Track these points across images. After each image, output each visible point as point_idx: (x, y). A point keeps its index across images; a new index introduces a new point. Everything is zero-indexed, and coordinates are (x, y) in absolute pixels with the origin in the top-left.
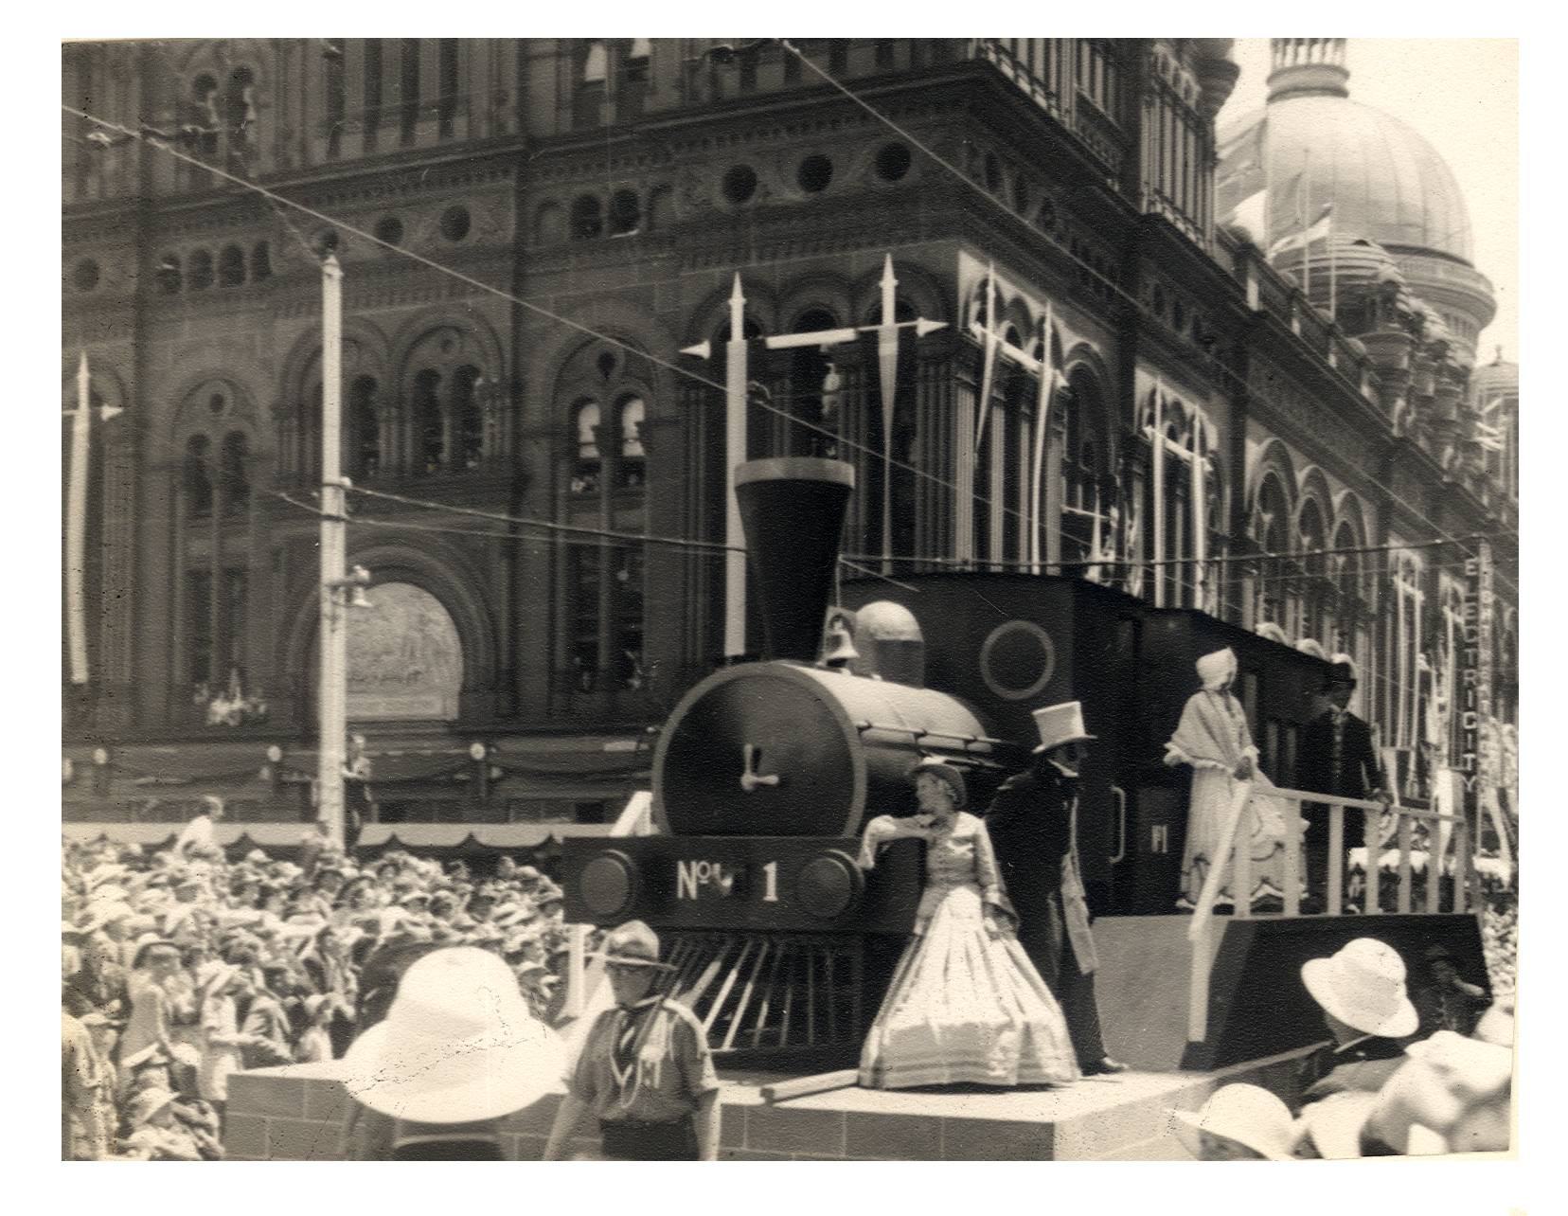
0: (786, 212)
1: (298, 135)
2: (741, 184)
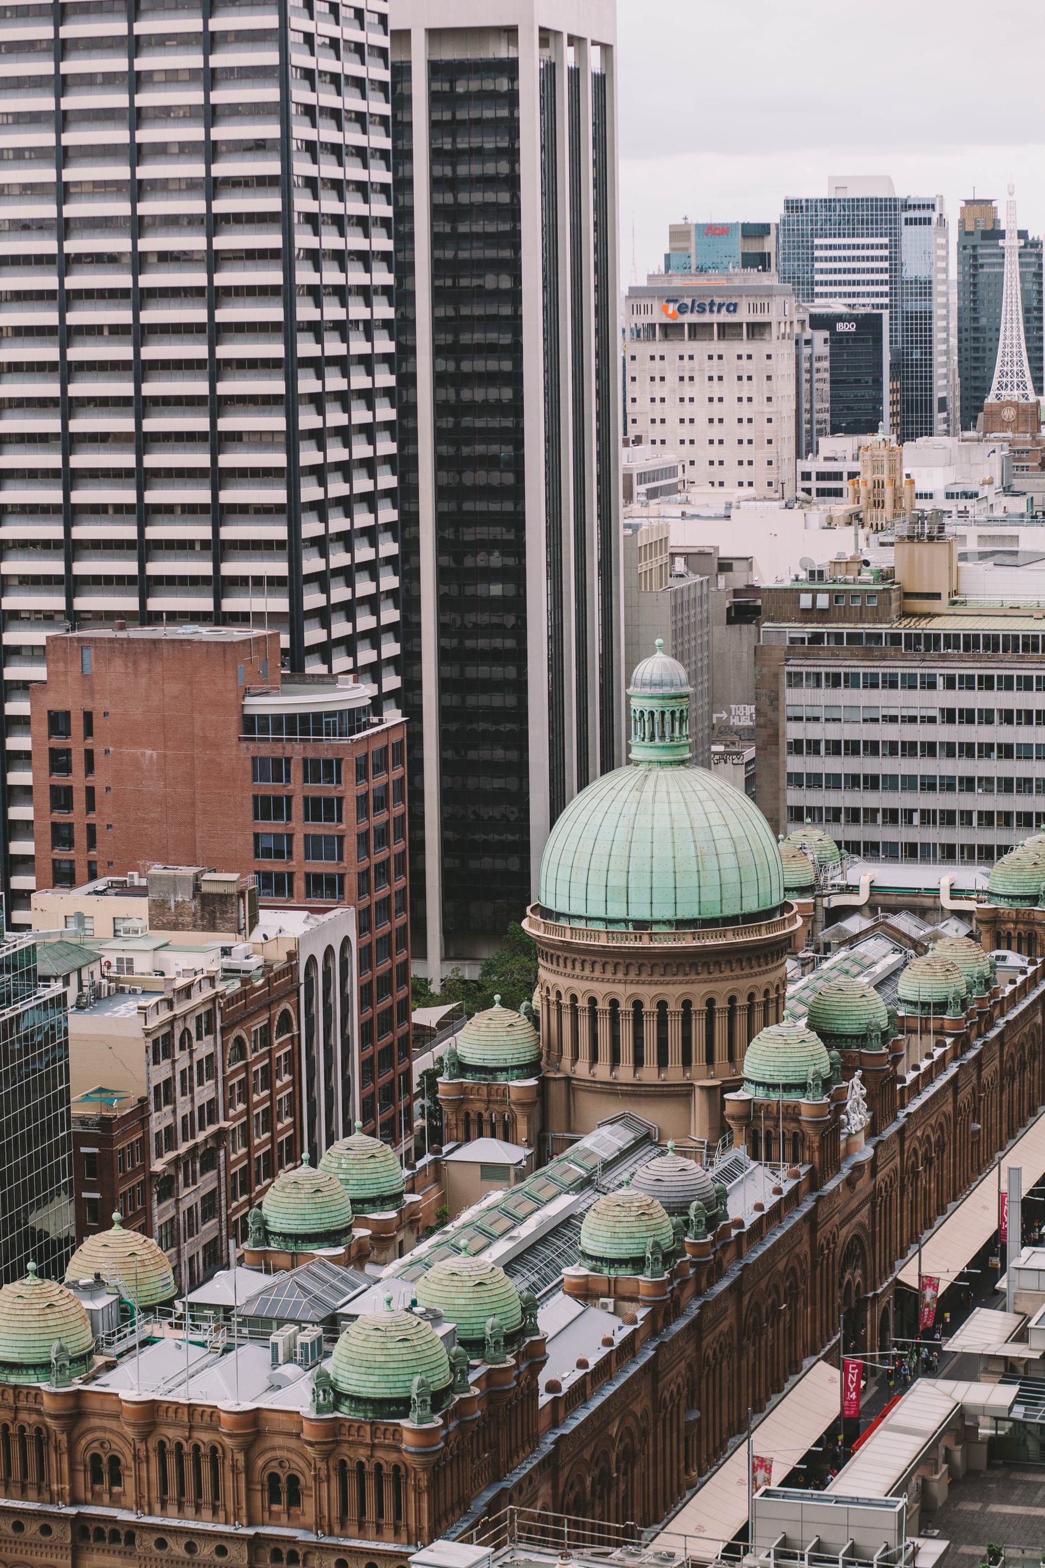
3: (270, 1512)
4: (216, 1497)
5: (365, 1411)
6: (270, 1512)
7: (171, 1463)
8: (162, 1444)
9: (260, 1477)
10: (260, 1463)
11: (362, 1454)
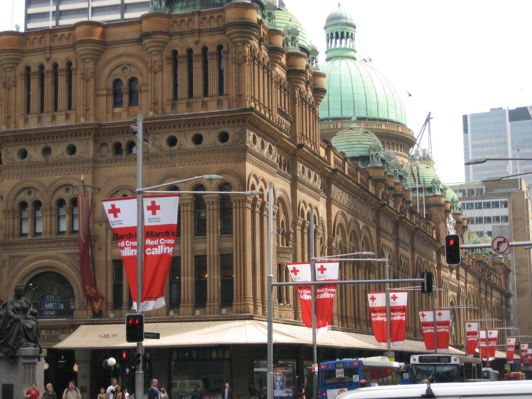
0: (189, 152)
1: (13, 117)
2: (172, 141)
3: (113, 114)
4: (70, 107)
5: (194, 6)
6: (113, 114)
7: (35, 83)
8: (28, 69)
9: (106, 83)
10: (106, 71)
11: (190, 42)
